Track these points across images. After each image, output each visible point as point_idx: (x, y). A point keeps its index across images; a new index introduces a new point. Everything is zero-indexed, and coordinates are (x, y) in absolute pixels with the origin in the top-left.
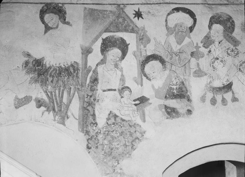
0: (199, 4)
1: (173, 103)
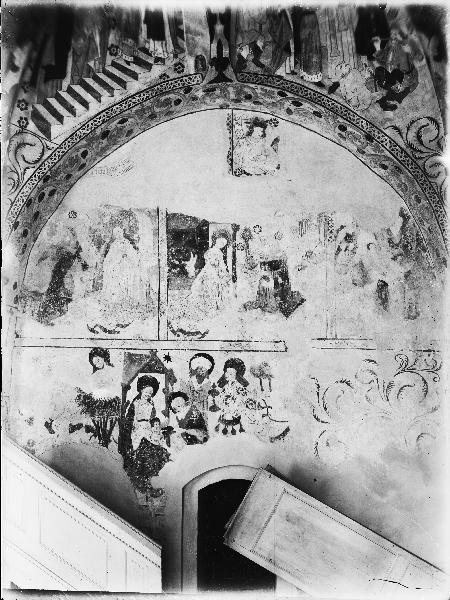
1: (192, 432)
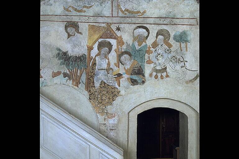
0: (152, 24)
1: (135, 77)
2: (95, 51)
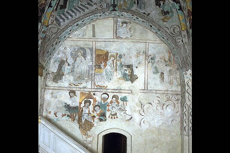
1: (101, 118)
2: (83, 105)
